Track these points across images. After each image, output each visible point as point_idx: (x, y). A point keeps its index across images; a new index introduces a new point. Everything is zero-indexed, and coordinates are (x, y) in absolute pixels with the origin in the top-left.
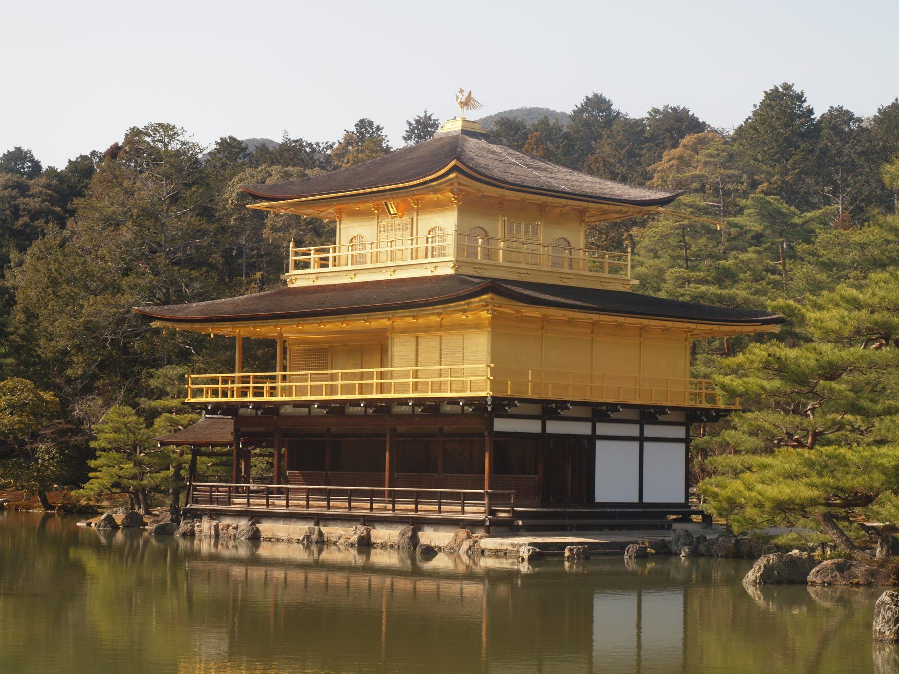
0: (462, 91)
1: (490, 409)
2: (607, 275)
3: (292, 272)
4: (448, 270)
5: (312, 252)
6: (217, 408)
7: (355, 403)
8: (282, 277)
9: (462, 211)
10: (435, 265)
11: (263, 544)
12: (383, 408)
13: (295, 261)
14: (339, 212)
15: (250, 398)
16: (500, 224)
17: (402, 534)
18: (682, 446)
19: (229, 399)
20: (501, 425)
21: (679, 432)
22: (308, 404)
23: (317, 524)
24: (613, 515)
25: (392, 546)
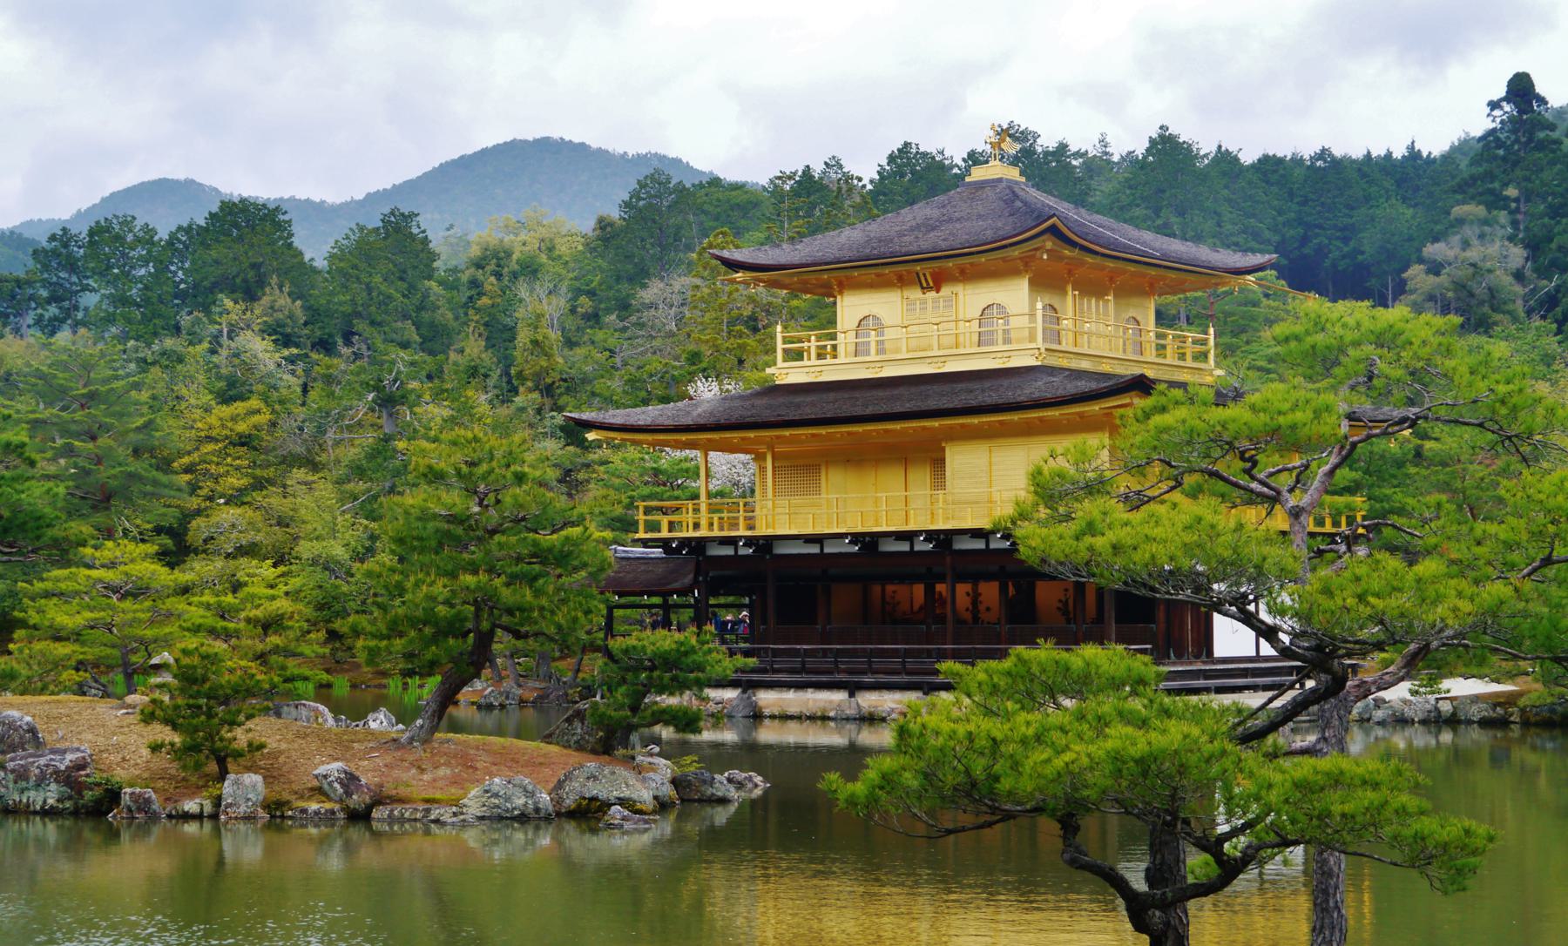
2: (1189, 363)
3: (780, 363)
4: (1032, 362)
6: (685, 542)
7: (908, 536)
8: (769, 371)
9: (1032, 283)
10: (1008, 354)
11: (767, 722)
12: (944, 539)
14: (844, 286)
15: (742, 532)
16: (1070, 298)
19: (684, 534)
23: (852, 695)
24: (1245, 673)
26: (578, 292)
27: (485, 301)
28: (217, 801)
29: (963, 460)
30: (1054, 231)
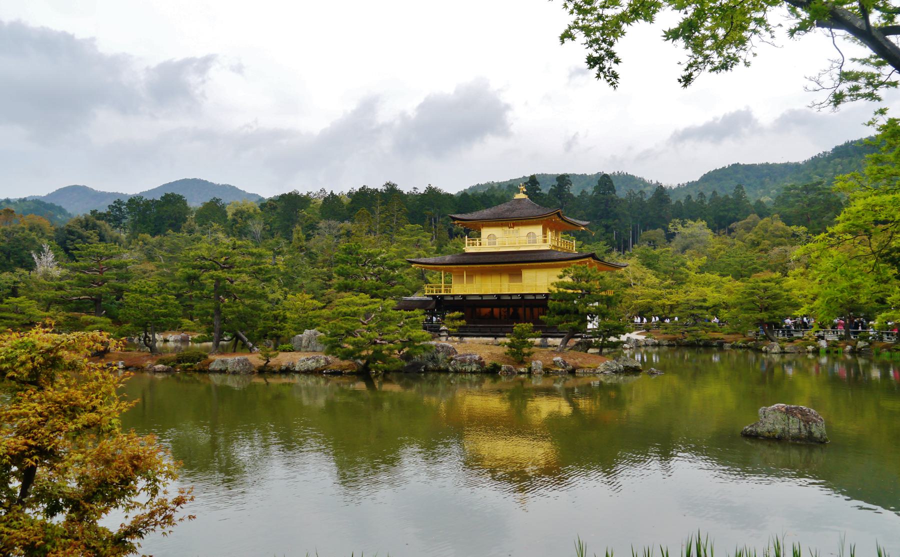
14: (483, 226)
17: (542, 341)
22: (481, 296)
26: (266, 224)
27: (238, 225)
28: (530, 369)
29: (527, 275)
30: (558, 214)
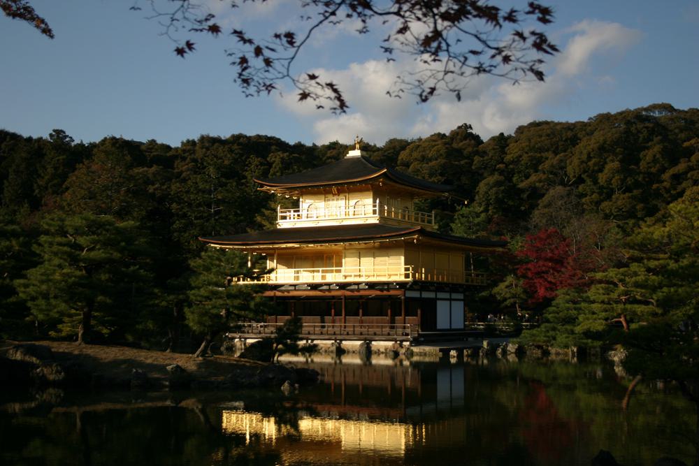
0: (357, 137)
1: (408, 286)
2: (426, 224)
3: (279, 221)
5: (292, 211)
13: (282, 216)
17: (361, 345)
18: (462, 303)
20: (410, 294)
21: (461, 296)
25: (354, 352)
